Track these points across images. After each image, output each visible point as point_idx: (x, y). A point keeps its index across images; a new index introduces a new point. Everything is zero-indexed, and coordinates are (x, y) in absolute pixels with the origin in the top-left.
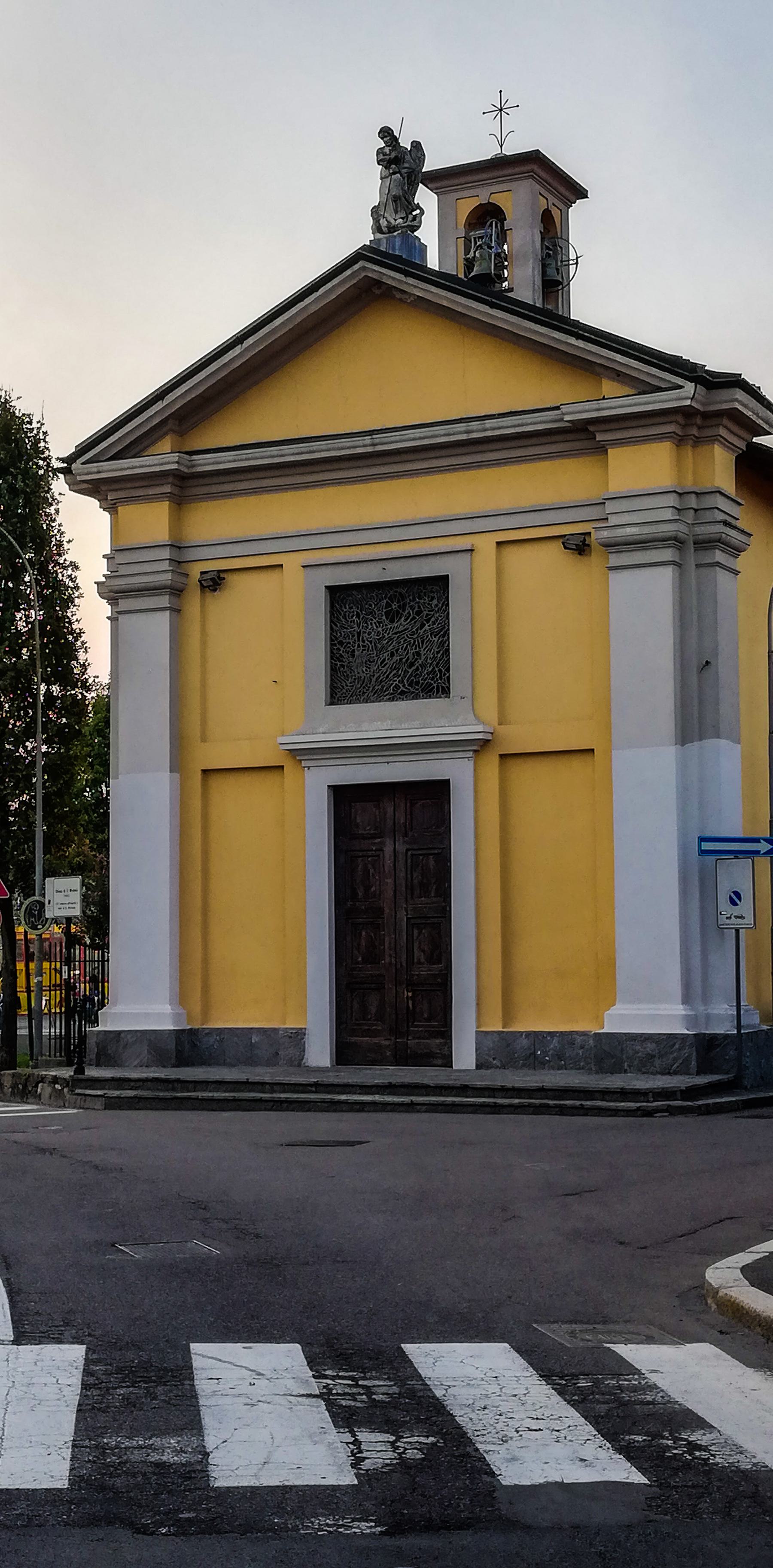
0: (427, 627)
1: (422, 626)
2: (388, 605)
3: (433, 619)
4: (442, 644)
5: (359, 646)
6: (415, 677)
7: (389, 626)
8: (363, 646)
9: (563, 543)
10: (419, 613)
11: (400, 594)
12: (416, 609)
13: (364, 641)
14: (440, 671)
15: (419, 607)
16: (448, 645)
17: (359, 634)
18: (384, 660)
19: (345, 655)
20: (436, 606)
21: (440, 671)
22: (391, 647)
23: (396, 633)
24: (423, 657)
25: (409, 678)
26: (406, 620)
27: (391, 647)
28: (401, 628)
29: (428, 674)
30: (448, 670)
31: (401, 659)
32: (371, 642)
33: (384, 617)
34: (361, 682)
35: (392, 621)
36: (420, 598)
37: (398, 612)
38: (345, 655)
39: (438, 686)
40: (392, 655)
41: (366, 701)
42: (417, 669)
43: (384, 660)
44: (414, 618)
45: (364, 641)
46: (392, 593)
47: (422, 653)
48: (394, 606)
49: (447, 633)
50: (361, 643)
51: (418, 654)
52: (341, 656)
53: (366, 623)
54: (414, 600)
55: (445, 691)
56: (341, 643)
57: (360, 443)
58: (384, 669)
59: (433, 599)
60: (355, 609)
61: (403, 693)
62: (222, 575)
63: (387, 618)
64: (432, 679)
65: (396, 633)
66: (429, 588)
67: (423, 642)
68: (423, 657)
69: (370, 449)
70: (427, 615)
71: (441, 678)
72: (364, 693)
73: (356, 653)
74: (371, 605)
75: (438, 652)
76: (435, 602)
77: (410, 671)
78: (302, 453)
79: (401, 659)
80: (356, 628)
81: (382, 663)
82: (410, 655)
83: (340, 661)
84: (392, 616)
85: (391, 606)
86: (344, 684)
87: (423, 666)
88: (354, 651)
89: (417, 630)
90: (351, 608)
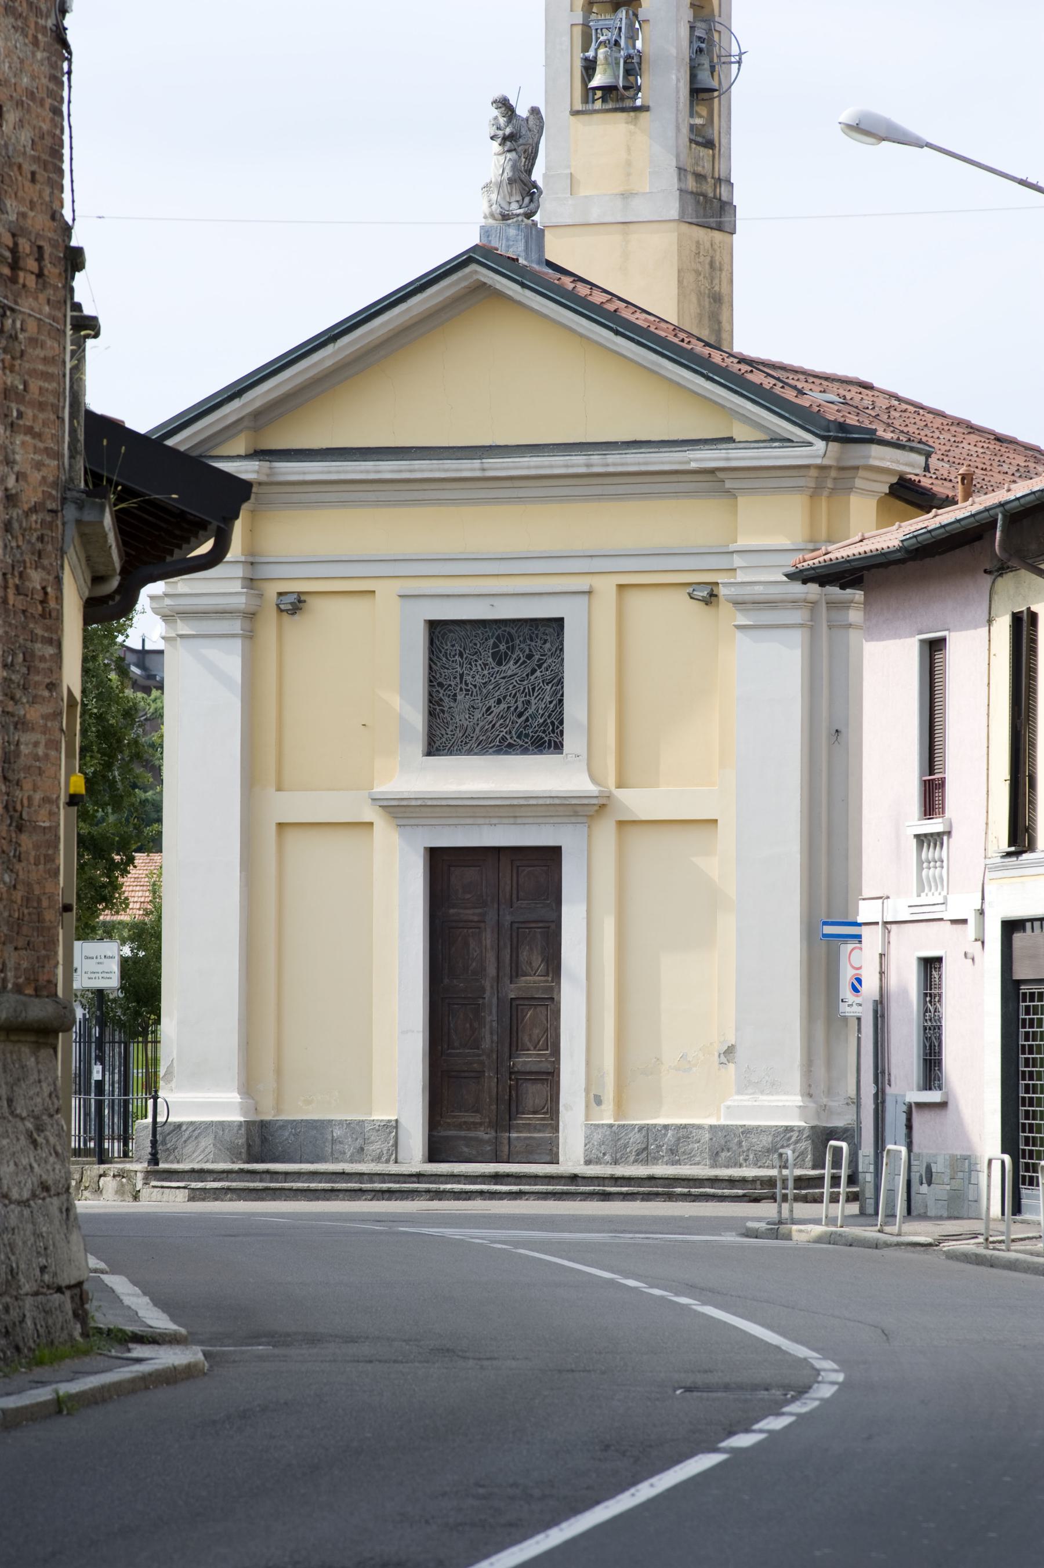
0: (538, 673)
1: (533, 671)
2: (495, 646)
3: (545, 665)
4: (555, 693)
5: (461, 690)
6: (524, 728)
7: (496, 669)
8: (467, 690)
9: (689, 594)
10: (530, 657)
11: (509, 633)
12: (527, 652)
13: (467, 685)
14: (553, 723)
15: (530, 650)
16: (562, 695)
17: (462, 676)
18: (490, 708)
19: (446, 699)
20: (550, 650)
21: (553, 723)
22: (498, 693)
23: (504, 678)
24: (534, 707)
25: (518, 730)
26: (516, 663)
27: (498, 693)
28: (510, 673)
29: (540, 726)
30: (561, 722)
31: (509, 708)
32: (475, 686)
33: (490, 659)
34: (463, 732)
35: (500, 664)
36: (532, 640)
37: (506, 654)
38: (446, 699)
39: (550, 741)
40: (499, 702)
41: (470, 752)
42: (527, 720)
43: (490, 708)
44: (524, 662)
45: (467, 685)
46: (500, 631)
47: (533, 702)
48: (502, 647)
49: (560, 682)
50: (464, 687)
51: (528, 702)
52: (441, 700)
53: (470, 664)
54: (525, 640)
55: (557, 747)
56: (440, 685)
57: (469, 466)
58: (490, 718)
59: (545, 642)
60: (457, 647)
61: (510, 746)
62: (303, 598)
63: (494, 660)
64: (544, 732)
65: (504, 678)
66: (542, 629)
67: (534, 689)
68: (534, 707)
69: (478, 474)
70: (540, 660)
71: (553, 731)
72: (466, 743)
73: (459, 698)
74: (475, 644)
75: (550, 702)
76: (548, 645)
77: (520, 721)
78: (400, 471)
79: (509, 708)
80: (459, 669)
81: (487, 710)
82: (520, 704)
83: (440, 705)
84: (500, 659)
85: (498, 647)
86: (443, 732)
87: (533, 716)
88: (455, 695)
89: (527, 675)
90: (453, 646)
